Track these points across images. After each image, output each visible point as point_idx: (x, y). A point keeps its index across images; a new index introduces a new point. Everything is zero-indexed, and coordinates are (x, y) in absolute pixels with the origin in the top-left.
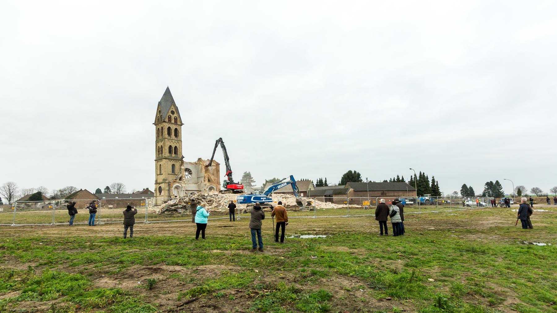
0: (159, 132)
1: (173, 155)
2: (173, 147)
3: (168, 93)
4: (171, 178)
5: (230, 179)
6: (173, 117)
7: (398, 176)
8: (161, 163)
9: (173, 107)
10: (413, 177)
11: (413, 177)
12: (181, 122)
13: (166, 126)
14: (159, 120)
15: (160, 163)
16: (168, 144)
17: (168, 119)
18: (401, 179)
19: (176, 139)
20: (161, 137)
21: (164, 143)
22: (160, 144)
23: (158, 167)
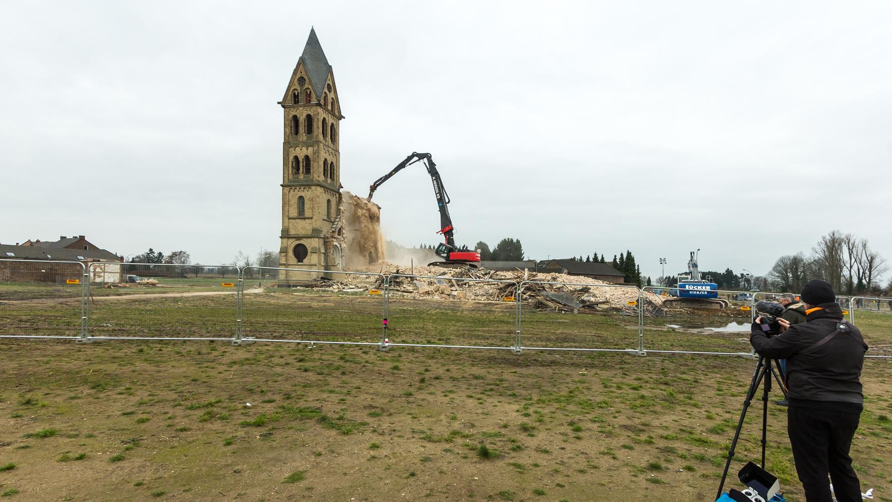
0: (293, 125)
1: (329, 181)
2: (330, 163)
3: (313, 41)
4: (326, 229)
5: (450, 241)
6: (331, 96)
7: (596, 255)
8: (307, 194)
9: (329, 77)
10: (625, 256)
11: (625, 256)
12: (340, 112)
13: (322, 114)
14: (294, 98)
15: (302, 194)
16: (323, 155)
17: (311, 102)
18: (600, 258)
19: (332, 146)
20: (303, 136)
21: (316, 153)
22: (301, 152)
23: (294, 201)
